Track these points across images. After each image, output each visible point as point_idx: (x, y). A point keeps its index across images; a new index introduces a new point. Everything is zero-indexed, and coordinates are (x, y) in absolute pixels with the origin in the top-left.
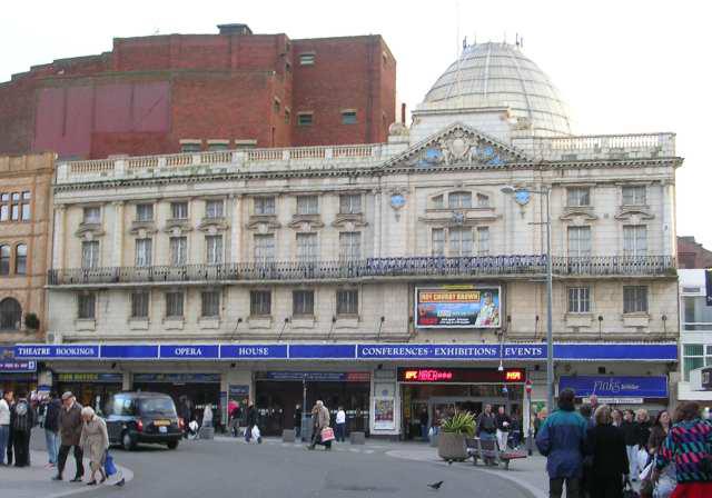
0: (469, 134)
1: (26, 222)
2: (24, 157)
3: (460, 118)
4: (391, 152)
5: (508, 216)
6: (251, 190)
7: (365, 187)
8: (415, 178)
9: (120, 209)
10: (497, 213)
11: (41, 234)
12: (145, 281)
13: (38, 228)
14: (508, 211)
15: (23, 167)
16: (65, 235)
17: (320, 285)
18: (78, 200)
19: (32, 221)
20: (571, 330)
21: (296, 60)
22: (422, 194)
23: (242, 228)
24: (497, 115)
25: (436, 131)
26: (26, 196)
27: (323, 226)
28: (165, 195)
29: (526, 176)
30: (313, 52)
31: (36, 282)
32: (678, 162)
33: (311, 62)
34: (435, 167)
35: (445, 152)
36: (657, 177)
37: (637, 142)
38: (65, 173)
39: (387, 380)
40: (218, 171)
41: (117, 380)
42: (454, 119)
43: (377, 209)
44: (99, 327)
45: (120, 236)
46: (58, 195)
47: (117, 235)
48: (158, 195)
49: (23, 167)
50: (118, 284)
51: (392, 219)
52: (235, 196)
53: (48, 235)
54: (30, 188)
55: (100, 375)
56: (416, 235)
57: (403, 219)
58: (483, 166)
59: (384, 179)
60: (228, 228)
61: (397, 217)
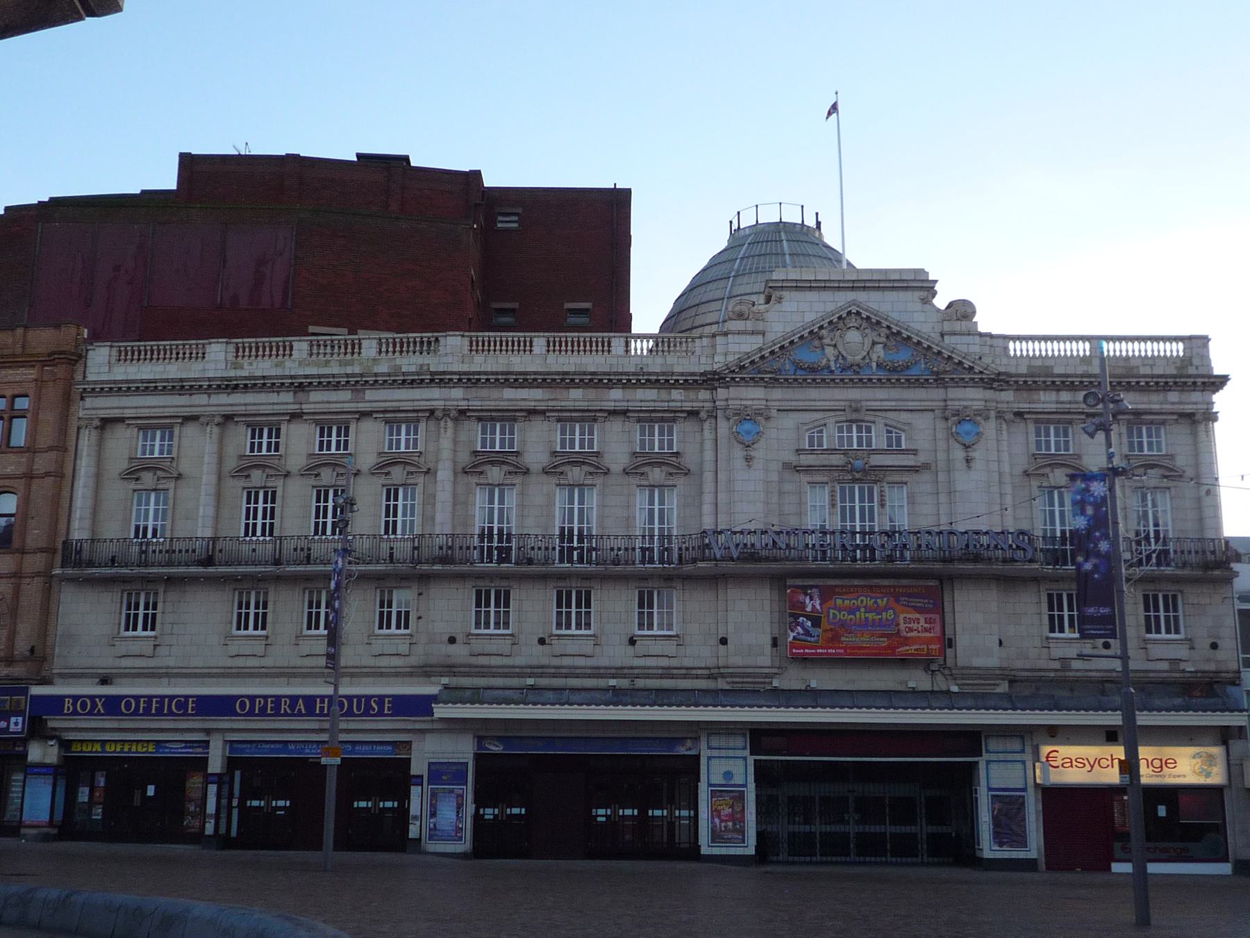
0: (871, 322)
1: (19, 450)
2: (20, 331)
3: (861, 296)
4: (732, 348)
5: (941, 465)
6: (476, 404)
7: (688, 406)
8: (777, 393)
9: (216, 430)
10: (922, 458)
11: (47, 474)
12: (266, 563)
13: (43, 463)
14: (941, 456)
15: (19, 350)
16: (98, 477)
17: (605, 578)
18: (128, 413)
19: (30, 449)
20: (1057, 665)
21: (491, 220)
22: (790, 421)
23: (455, 474)
24: (917, 294)
25: (809, 317)
26: (22, 403)
27: (607, 472)
28: (306, 408)
29: (974, 397)
30: (520, 210)
31: (35, 562)
32: (1222, 381)
33: (515, 225)
34: (814, 375)
35: (830, 351)
36: (1188, 408)
37: (1149, 349)
38: (101, 362)
39: (731, 753)
40: (413, 369)
41: (197, 752)
42: (851, 296)
43: (709, 445)
44: (162, 651)
45: (213, 479)
46: (89, 402)
47: (208, 478)
48: (293, 408)
49: (19, 350)
50: (211, 570)
51: (739, 463)
52: (446, 413)
53: (62, 477)
54: (31, 389)
55: (1174, 661)
56: (781, 493)
57: (758, 464)
58: (894, 375)
59: (722, 393)
60: (428, 472)
61: (748, 459)
